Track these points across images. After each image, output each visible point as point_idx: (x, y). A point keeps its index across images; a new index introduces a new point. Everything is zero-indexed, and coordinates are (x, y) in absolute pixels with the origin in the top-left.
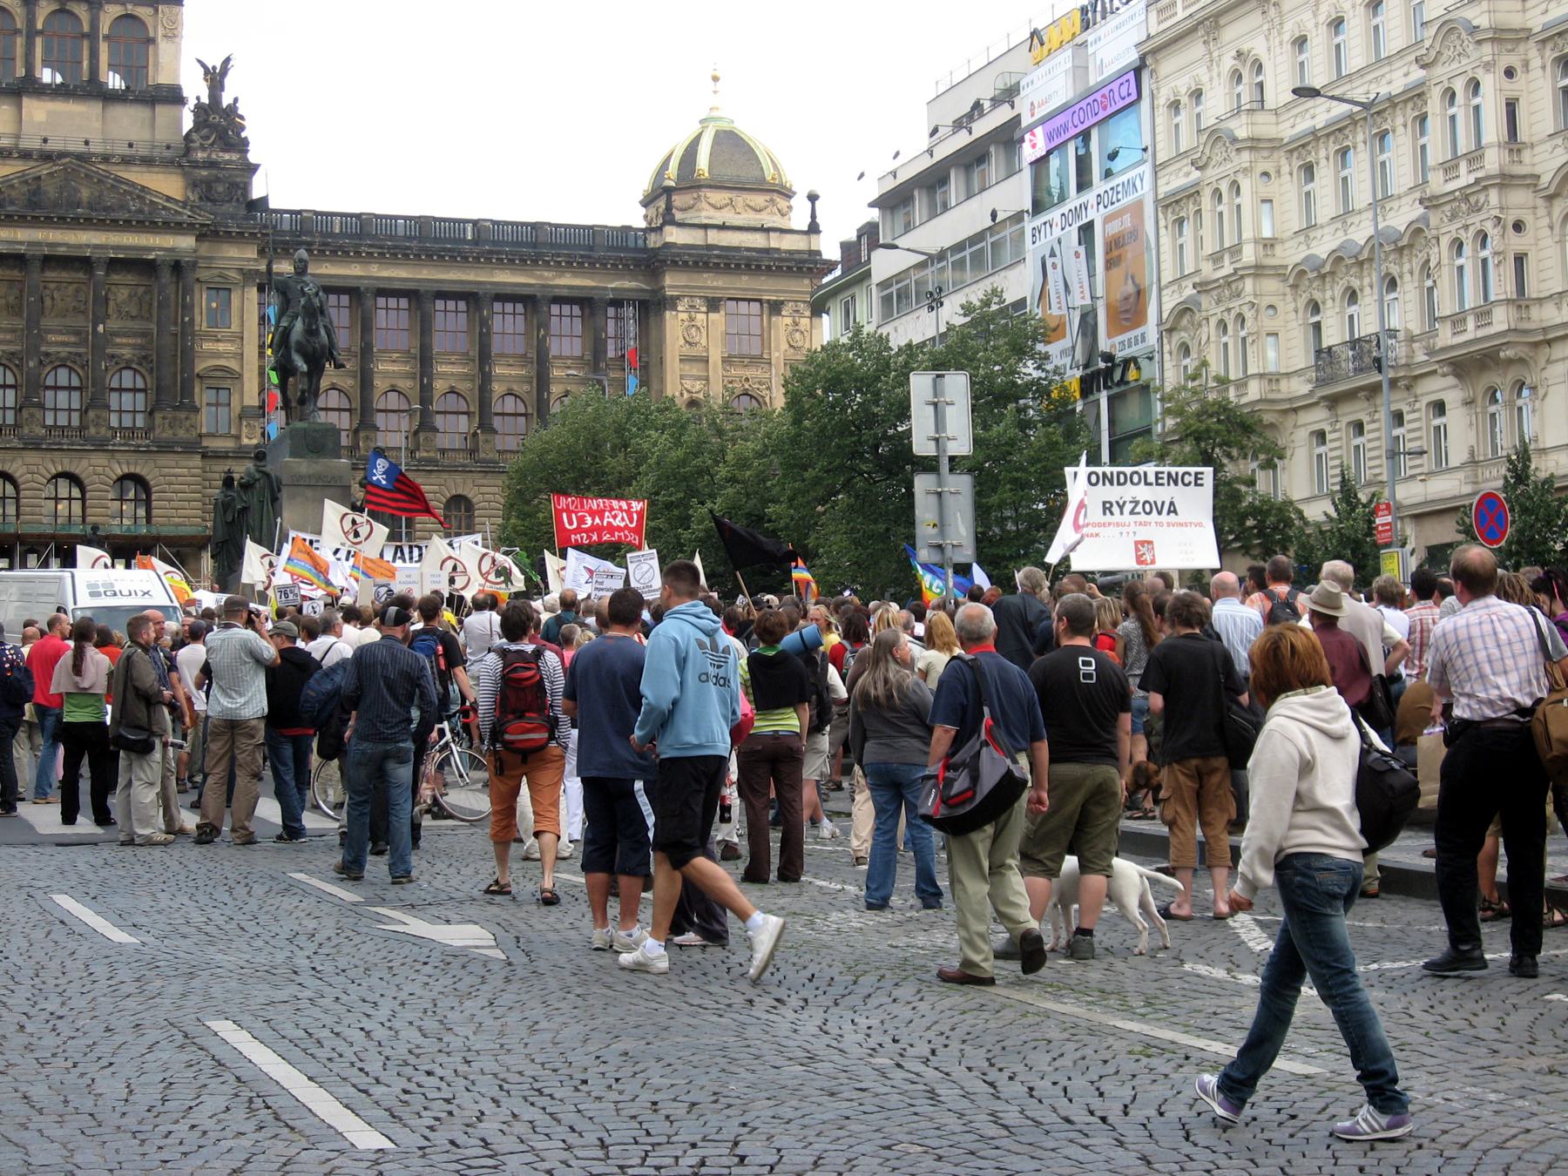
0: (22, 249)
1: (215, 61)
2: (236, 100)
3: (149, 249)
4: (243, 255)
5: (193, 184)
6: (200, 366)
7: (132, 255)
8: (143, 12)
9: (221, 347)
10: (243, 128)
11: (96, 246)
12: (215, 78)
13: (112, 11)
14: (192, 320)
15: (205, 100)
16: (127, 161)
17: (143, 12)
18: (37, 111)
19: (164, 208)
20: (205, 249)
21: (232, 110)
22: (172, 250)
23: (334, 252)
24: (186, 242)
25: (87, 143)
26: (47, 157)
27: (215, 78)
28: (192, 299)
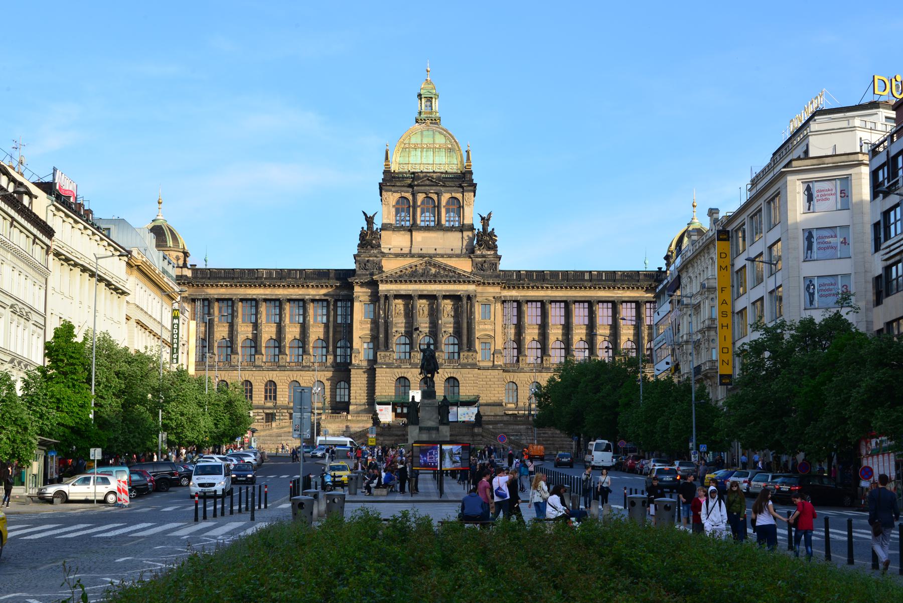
0: (410, 293)
1: (485, 215)
2: (493, 229)
3: (459, 291)
4: (494, 291)
5: (475, 265)
6: (477, 334)
7: (452, 293)
8: (459, 196)
9: (486, 327)
10: (496, 240)
11: (438, 291)
12: (485, 221)
13: (445, 197)
14: (475, 318)
15: (481, 230)
16: (450, 256)
17: (459, 196)
18: (418, 236)
19: (463, 275)
20: (480, 289)
21: (492, 234)
22: (467, 291)
23: (533, 287)
24: (471, 288)
25: (436, 250)
26: (421, 256)
27: (485, 221)
28: (475, 309)
